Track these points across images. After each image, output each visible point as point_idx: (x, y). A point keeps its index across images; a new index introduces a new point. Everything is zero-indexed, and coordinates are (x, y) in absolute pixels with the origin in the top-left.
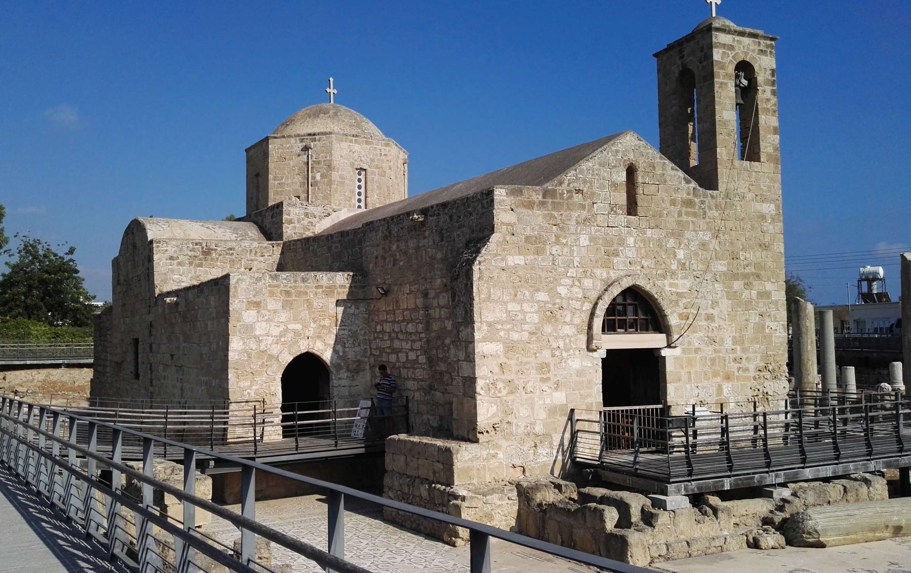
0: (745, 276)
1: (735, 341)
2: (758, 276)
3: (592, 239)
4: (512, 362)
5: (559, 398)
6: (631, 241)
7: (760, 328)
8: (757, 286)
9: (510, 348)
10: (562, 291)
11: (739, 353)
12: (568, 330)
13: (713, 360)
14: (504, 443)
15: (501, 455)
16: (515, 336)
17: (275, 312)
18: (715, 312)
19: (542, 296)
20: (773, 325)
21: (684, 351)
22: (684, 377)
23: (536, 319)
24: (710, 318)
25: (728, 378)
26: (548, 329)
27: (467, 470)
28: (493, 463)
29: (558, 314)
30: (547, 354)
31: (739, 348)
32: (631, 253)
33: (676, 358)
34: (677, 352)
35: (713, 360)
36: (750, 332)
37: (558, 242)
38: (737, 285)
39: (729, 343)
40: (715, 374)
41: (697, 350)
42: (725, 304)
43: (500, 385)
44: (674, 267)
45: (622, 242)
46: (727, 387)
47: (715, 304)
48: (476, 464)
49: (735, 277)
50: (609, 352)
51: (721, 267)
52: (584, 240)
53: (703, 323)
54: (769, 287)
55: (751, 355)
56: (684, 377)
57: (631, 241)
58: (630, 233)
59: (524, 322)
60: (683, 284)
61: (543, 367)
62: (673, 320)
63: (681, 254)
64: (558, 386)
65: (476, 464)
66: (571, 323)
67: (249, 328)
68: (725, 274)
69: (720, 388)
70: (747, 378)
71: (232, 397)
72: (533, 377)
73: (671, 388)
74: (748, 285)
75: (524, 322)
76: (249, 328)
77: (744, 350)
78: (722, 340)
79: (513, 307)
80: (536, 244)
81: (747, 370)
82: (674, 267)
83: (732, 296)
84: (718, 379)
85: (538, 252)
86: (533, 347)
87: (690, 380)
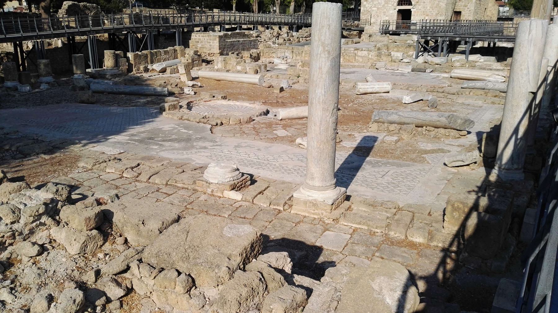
4: (378, 11)
5: (387, 18)
9: (378, 9)
12: (390, 5)
13: (424, 12)
14: (375, 26)
15: (374, 28)
16: (379, 7)
17: (370, 2)
21: (416, 10)
22: (416, 15)
23: (384, 3)
26: (386, 5)
27: (367, 30)
28: (372, 29)
29: (389, 2)
30: (385, 10)
31: (431, 9)
33: (414, 11)
34: (415, 10)
35: (424, 12)
36: (435, 5)
39: (428, 8)
40: (424, 15)
41: (420, 9)
43: (376, 16)
48: (369, 29)
50: (399, 10)
55: (434, 11)
56: (416, 15)
59: (381, 4)
61: (384, 12)
62: (413, 3)
65: (369, 29)
66: (391, 4)
67: (365, 5)
70: (433, 16)
71: (361, 19)
72: (383, 14)
73: (412, 18)
75: (381, 4)
76: (365, 5)
77: (432, 10)
78: (427, 8)
81: (433, 14)
84: (424, 16)
86: (383, 8)
87: (417, 15)
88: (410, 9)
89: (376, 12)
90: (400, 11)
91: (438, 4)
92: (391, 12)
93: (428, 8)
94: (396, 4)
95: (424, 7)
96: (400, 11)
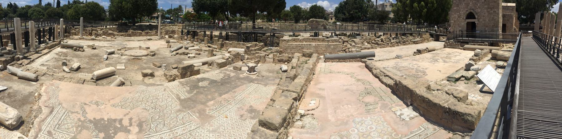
0: (491, 8)
1: (488, 20)
2: (493, 8)
3: (465, 4)
5: (460, 29)
6: (471, 3)
7: (493, 18)
8: (493, 10)
9: (455, 21)
10: (461, 12)
11: (489, 23)
12: (462, 19)
13: (484, 24)
18: (485, 15)
19: (458, 14)
20: (496, 17)
23: (457, 17)
24: (484, 16)
25: (487, 27)
26: (459, 18)
30: (458, 22)
31: (489, 22)
32: (470, 5)
37: (460, 5)
38: (489, 10)
39: (487, 20)
40: (484, 26)
41: (481, 22)
42: (487, 14)
44: (478, 7)
45: (469, 3)
46: (486, 29)
47: (485, 13)
49: (489, 8)
51: (486, 6)
52: (464, 4)
53: (482, 17)
54: (496, 10)
57: (471, 3)
58: (471, 2)
60: (479, 10)
62: (476, 17)
63: (479, 5)
64: (460, 27)
68: (487, 8)
69: (485, 29)
74: (492, 10)
77: (490, 22)
79: (455, 15)
80: (458, 6)
82: (478, 7)
83: (488, 12)
85: (458, 6)
88: (475, 22)
89: (453, 24)
90: (468, 23)
91: (493, 18)
92: (463, 24)
93: (487, 20)
94: (465, 18)
95: (484, 20)
96: (468, 23)
